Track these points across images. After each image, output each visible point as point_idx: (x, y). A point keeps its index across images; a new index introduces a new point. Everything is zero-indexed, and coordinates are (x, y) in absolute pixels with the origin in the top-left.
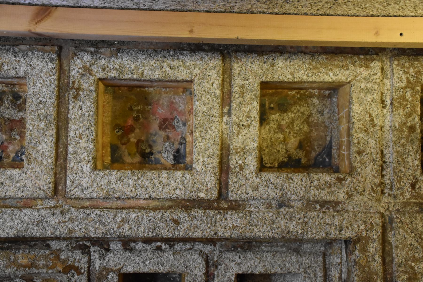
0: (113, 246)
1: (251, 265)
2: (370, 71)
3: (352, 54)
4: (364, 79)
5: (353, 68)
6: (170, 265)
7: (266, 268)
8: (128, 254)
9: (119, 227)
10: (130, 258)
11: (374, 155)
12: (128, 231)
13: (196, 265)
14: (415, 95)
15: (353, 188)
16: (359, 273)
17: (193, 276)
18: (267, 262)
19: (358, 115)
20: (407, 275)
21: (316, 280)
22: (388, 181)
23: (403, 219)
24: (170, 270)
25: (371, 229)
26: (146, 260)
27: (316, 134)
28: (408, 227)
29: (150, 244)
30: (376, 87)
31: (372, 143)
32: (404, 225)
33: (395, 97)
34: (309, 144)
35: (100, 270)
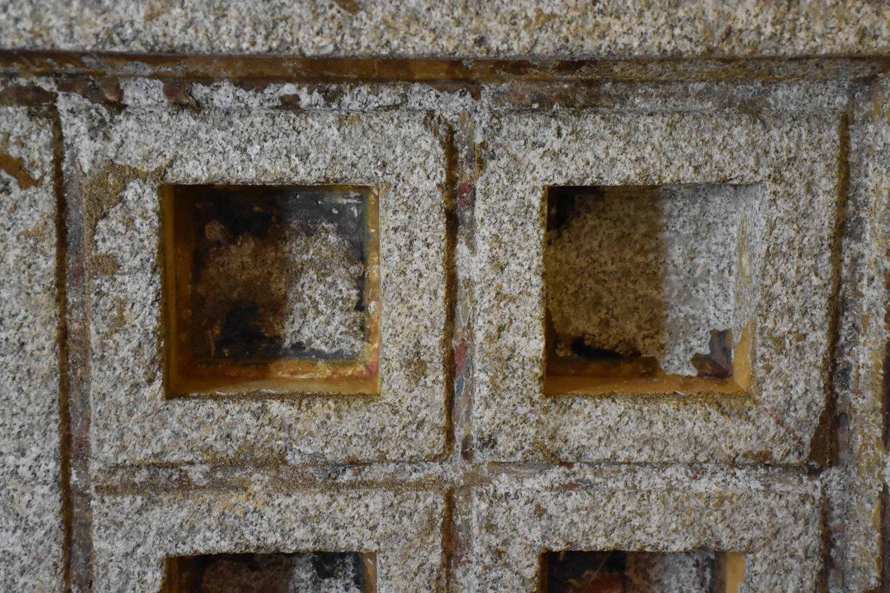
0: (132, 94)
1: (597, 157)
6: (328, 157)
7: (645, 166)
8: (187, 121)
9: (151, 17)
10: (195, 135)
12: (184, 30)
13: (414, 160)
17: (406, 195)
18: (649, 148)
21: (811, 202)
24: (329, 173)
26: (249, 141)
29: (260, 90)
35: (96, 171)
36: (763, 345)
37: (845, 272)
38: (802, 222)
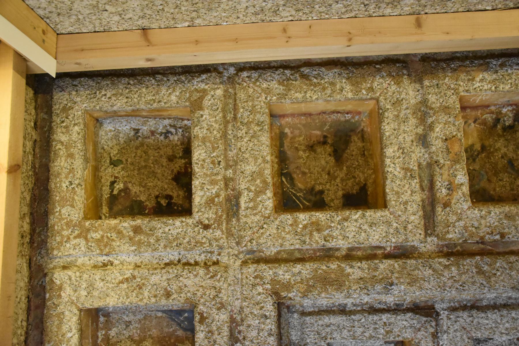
2: (65, 285)
3: (45, 308)
4: (76, 291)
5: (62, 307)
11: (171, 276)
14: (96, 227)
15: (211, 302)
16: (316, 291)
19: (121, 298)
20: (314, 233)
21: (333, 325)
22: (203, 256)
23: (247, 238)
25: (262, 278)
27: (154, 330)
28: (257, 233)
30: (85, 276)
31: (155, 279)
32: (255, 237)
33: (98, 251)
34: (167, 339)
36: (389, 338)
37: (359, 308)
38: (341, 327)
